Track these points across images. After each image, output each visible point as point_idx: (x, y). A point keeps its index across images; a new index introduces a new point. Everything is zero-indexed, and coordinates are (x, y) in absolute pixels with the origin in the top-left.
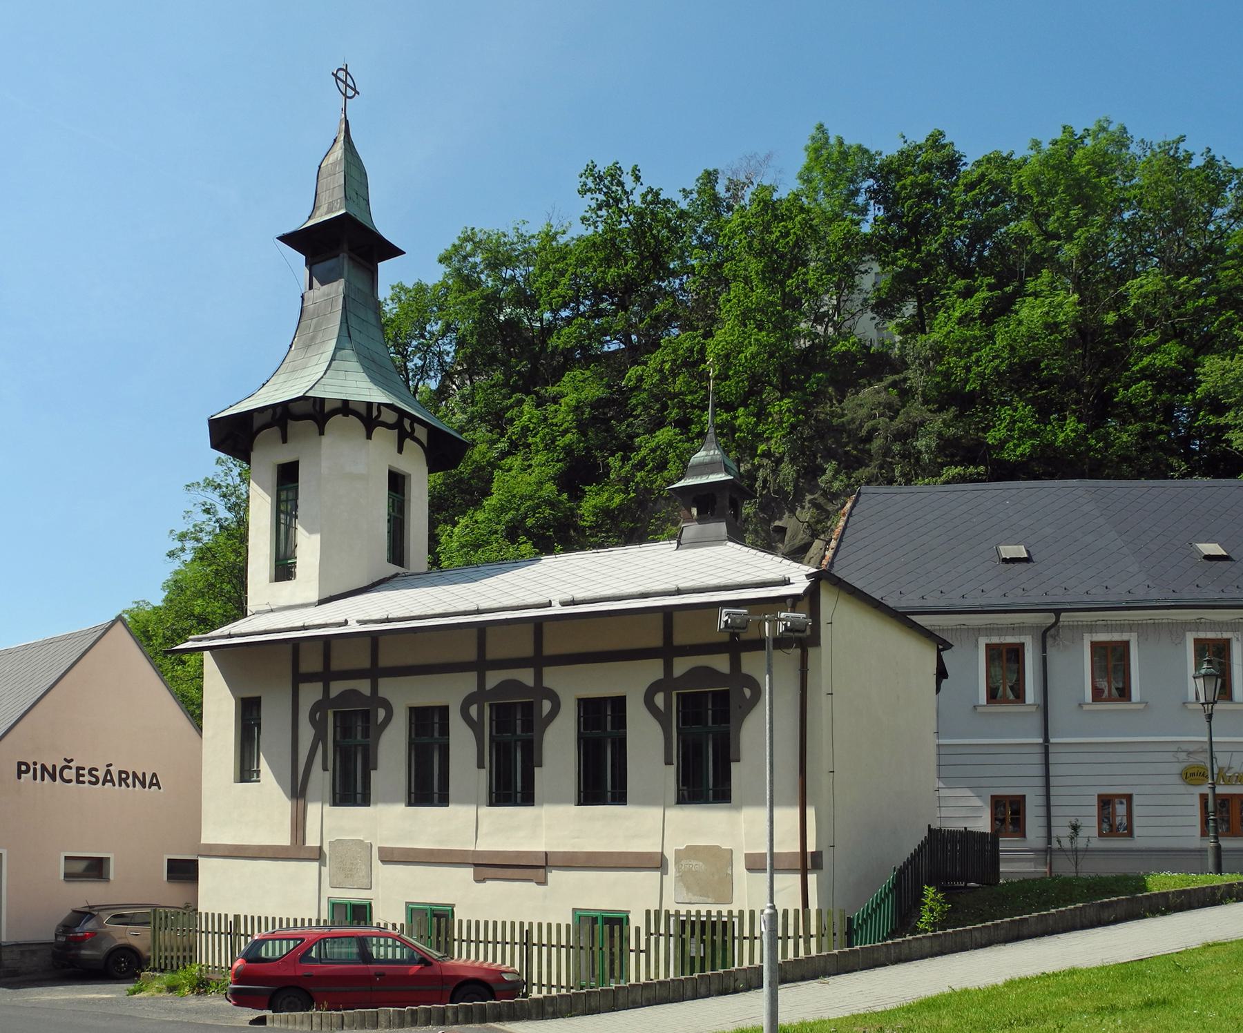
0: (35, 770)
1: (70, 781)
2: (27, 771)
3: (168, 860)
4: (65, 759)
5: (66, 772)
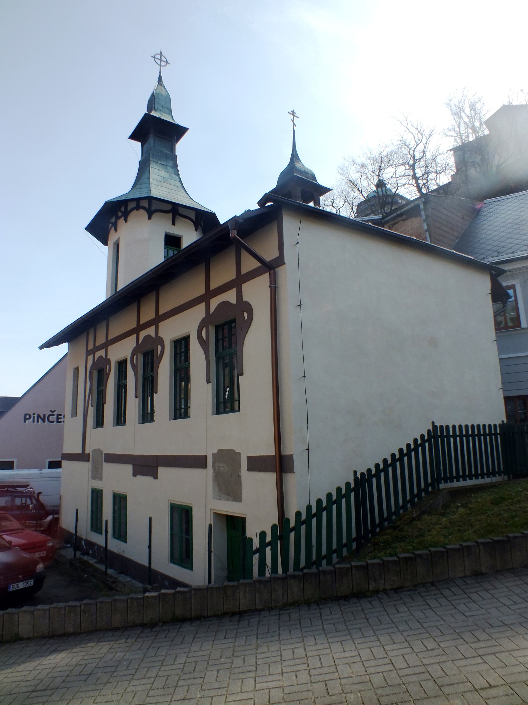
0: (34, 417)
1: (53, 422)
2: (29, 418)
3: (13, 462)
4: (51, 411)
5: (51, 417)
